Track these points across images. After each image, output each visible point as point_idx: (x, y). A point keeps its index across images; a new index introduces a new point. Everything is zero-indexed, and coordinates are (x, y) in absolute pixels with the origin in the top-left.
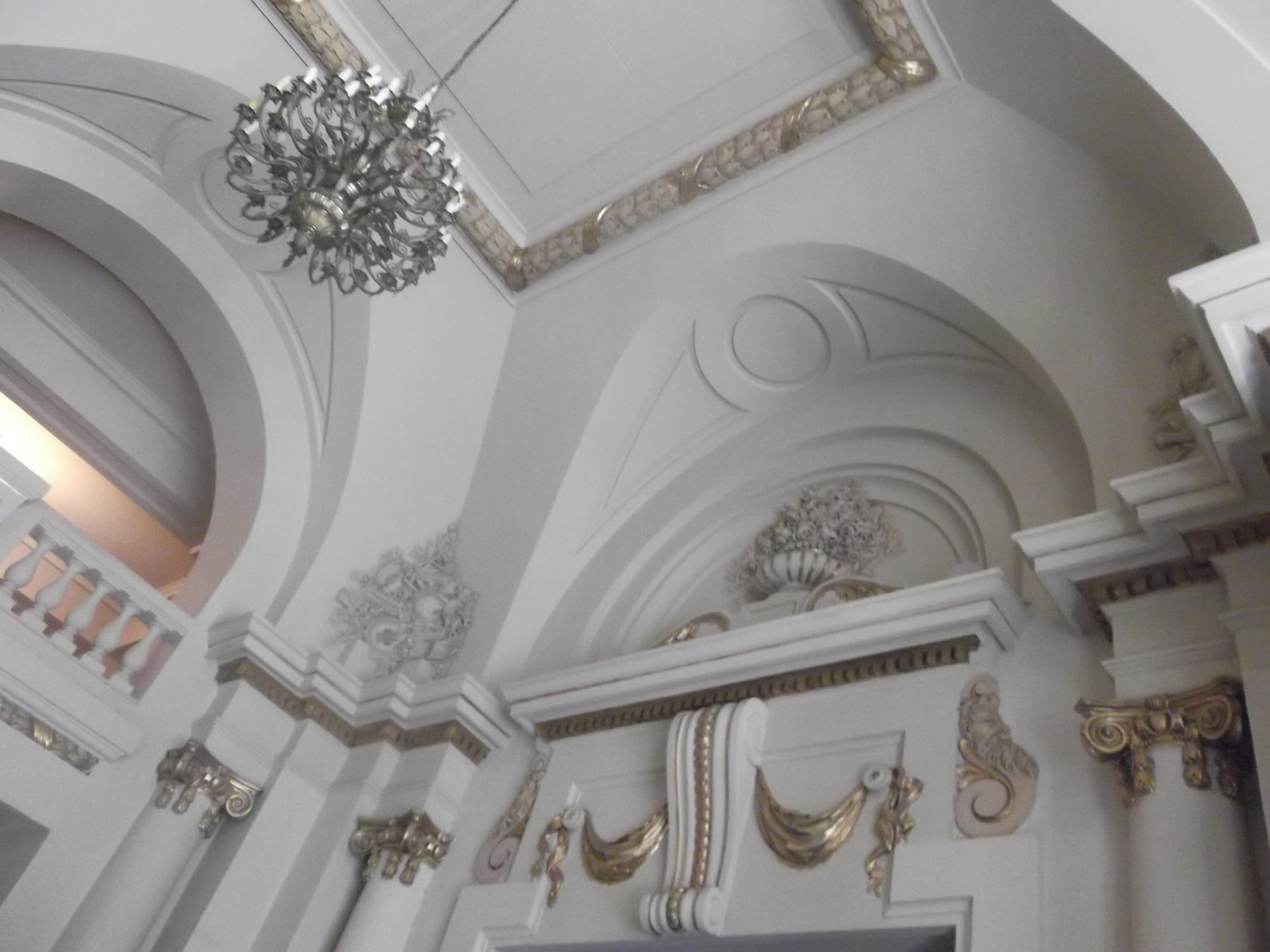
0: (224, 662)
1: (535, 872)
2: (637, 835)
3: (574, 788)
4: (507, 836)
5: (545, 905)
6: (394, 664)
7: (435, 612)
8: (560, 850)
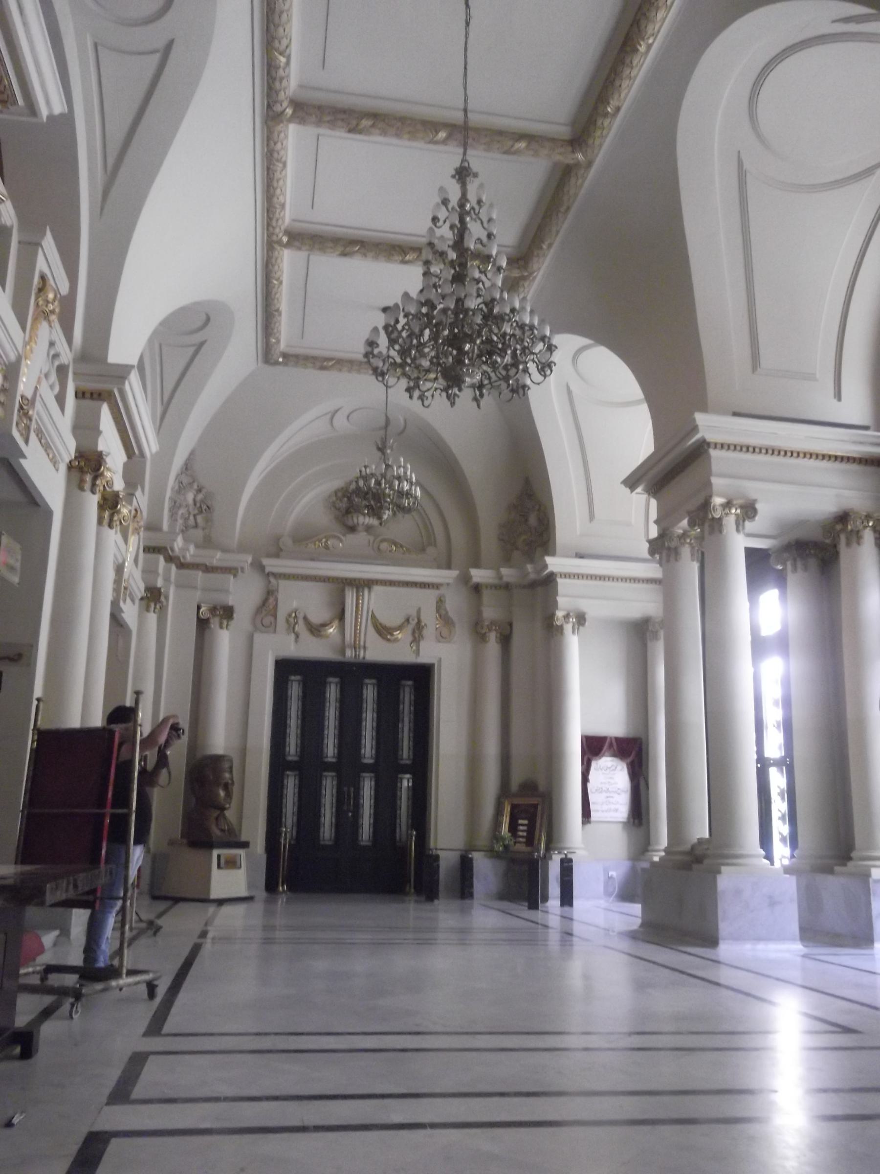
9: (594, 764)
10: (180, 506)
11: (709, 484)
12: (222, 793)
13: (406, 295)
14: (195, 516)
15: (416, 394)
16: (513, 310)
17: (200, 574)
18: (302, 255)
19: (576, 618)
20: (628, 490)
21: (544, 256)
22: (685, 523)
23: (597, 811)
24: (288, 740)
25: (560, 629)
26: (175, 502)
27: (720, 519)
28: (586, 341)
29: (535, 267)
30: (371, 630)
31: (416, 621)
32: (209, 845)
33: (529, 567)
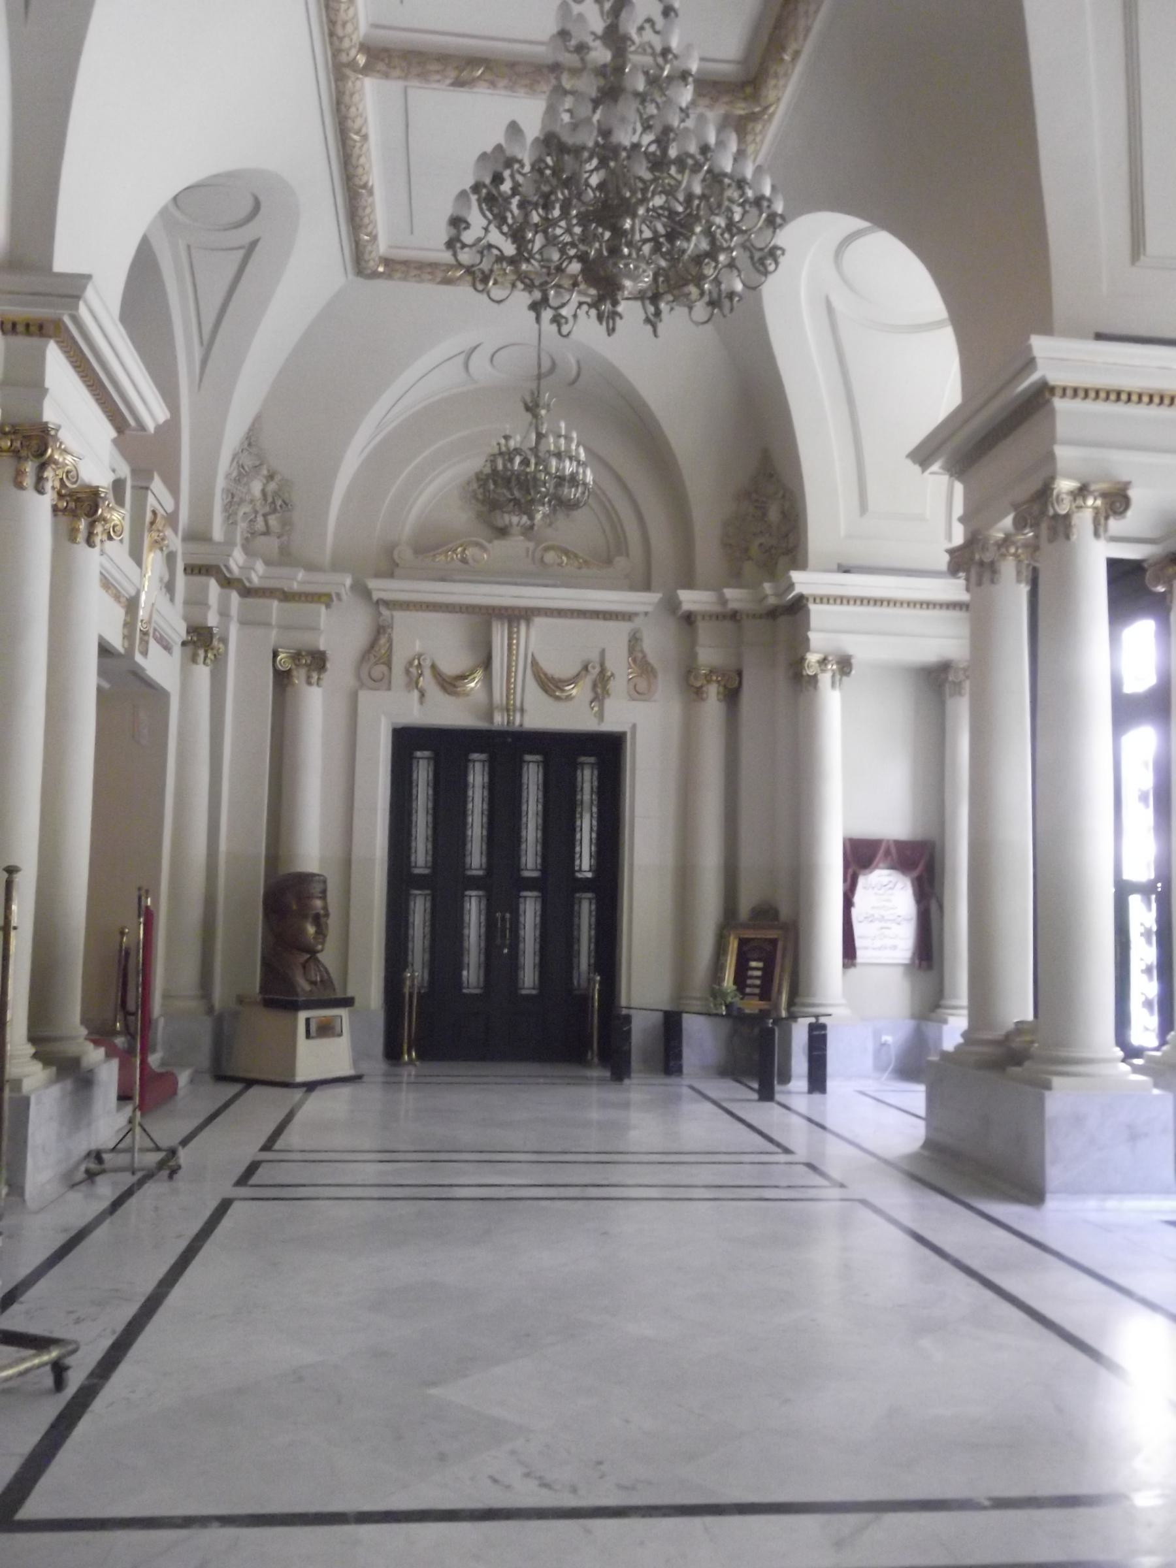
4: (376, 664)
9: (862, 881)
10: (242, 501)
11: (1050, 457)
12: (311, 930)
13: (514, 129)
14: (265, 516)
15: (547, 314)
16: (705, 149)
17: (275, 604)
18: (394, 87)
19: (838, 663)
20: (917, 468)
21: (787, 75)
22: (1008, 522)
23: (866, 948)
24: (413, 844)
25: (814, 679)
26: (233, 496)
27: (1067, 517)
28: (858, 223)
29: (772, 95)
30: (532, 686)
31: (598, 669)
32: (293, 1006)
33: (767, 587)
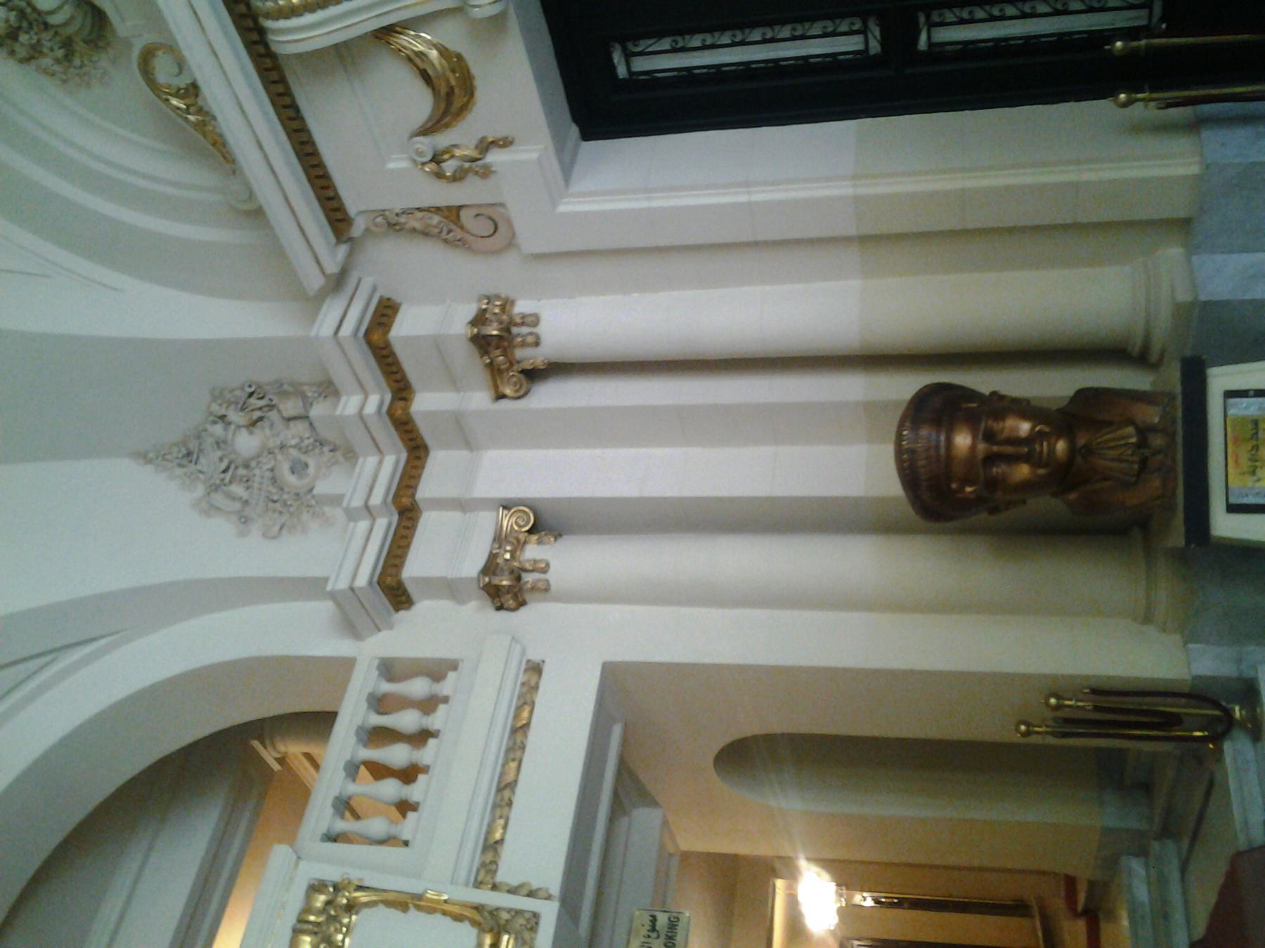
0: (390, 608)
1: (486, 172)
2: (416, 63)
3: (391, 165)
5: (513, 148)
6: (326, 449)
7: (251, 433)
8: (458, 153)
